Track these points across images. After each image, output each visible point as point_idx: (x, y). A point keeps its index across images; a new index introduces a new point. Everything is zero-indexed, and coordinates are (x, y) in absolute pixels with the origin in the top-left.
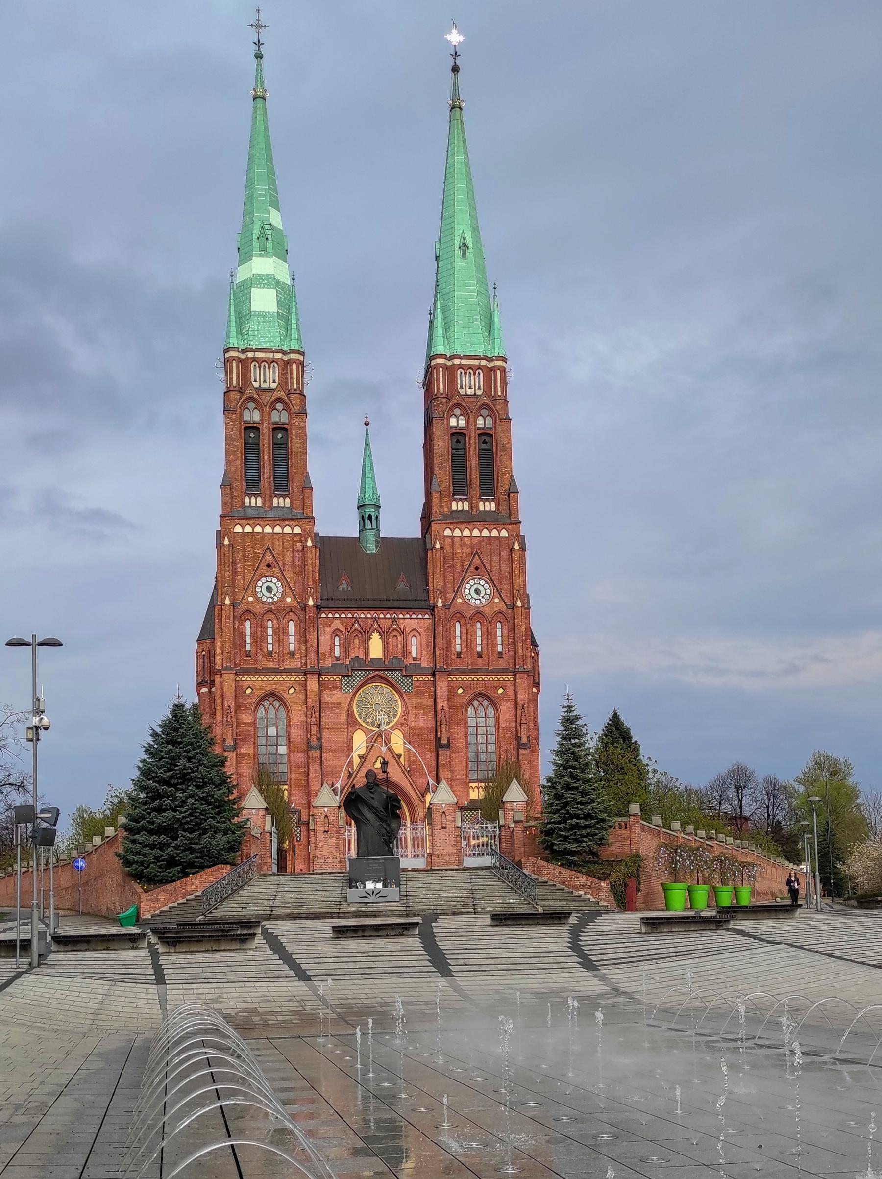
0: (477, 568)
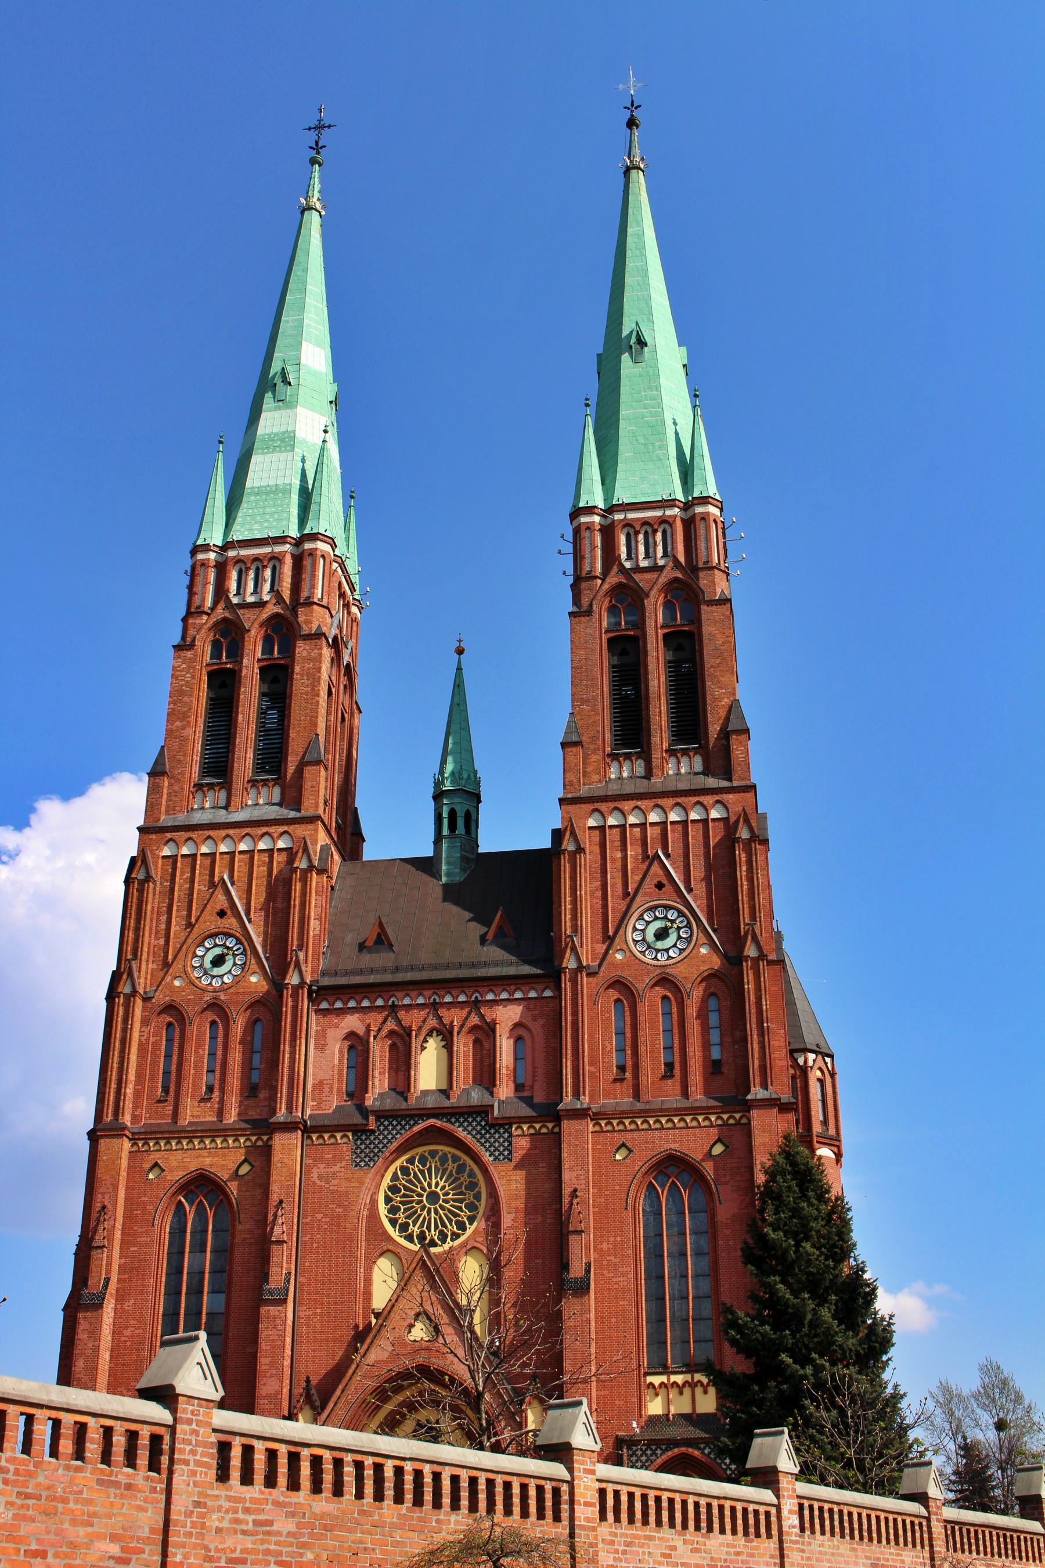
0: (660, 886)
